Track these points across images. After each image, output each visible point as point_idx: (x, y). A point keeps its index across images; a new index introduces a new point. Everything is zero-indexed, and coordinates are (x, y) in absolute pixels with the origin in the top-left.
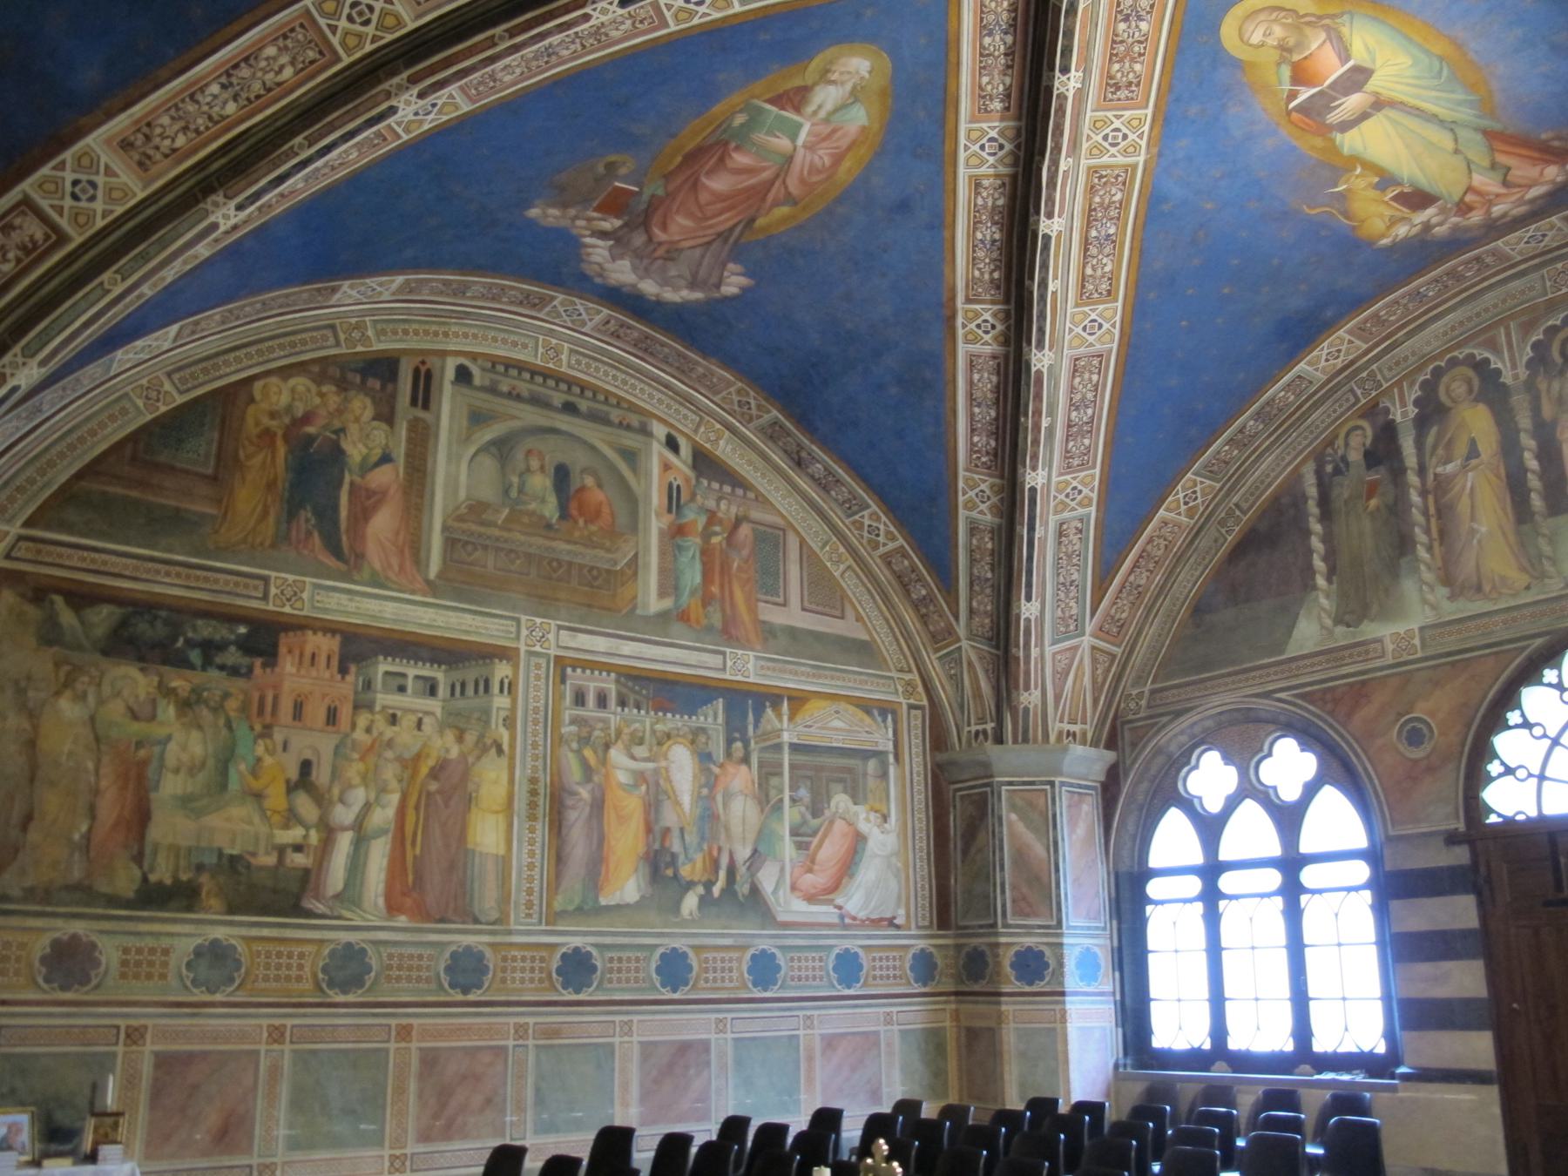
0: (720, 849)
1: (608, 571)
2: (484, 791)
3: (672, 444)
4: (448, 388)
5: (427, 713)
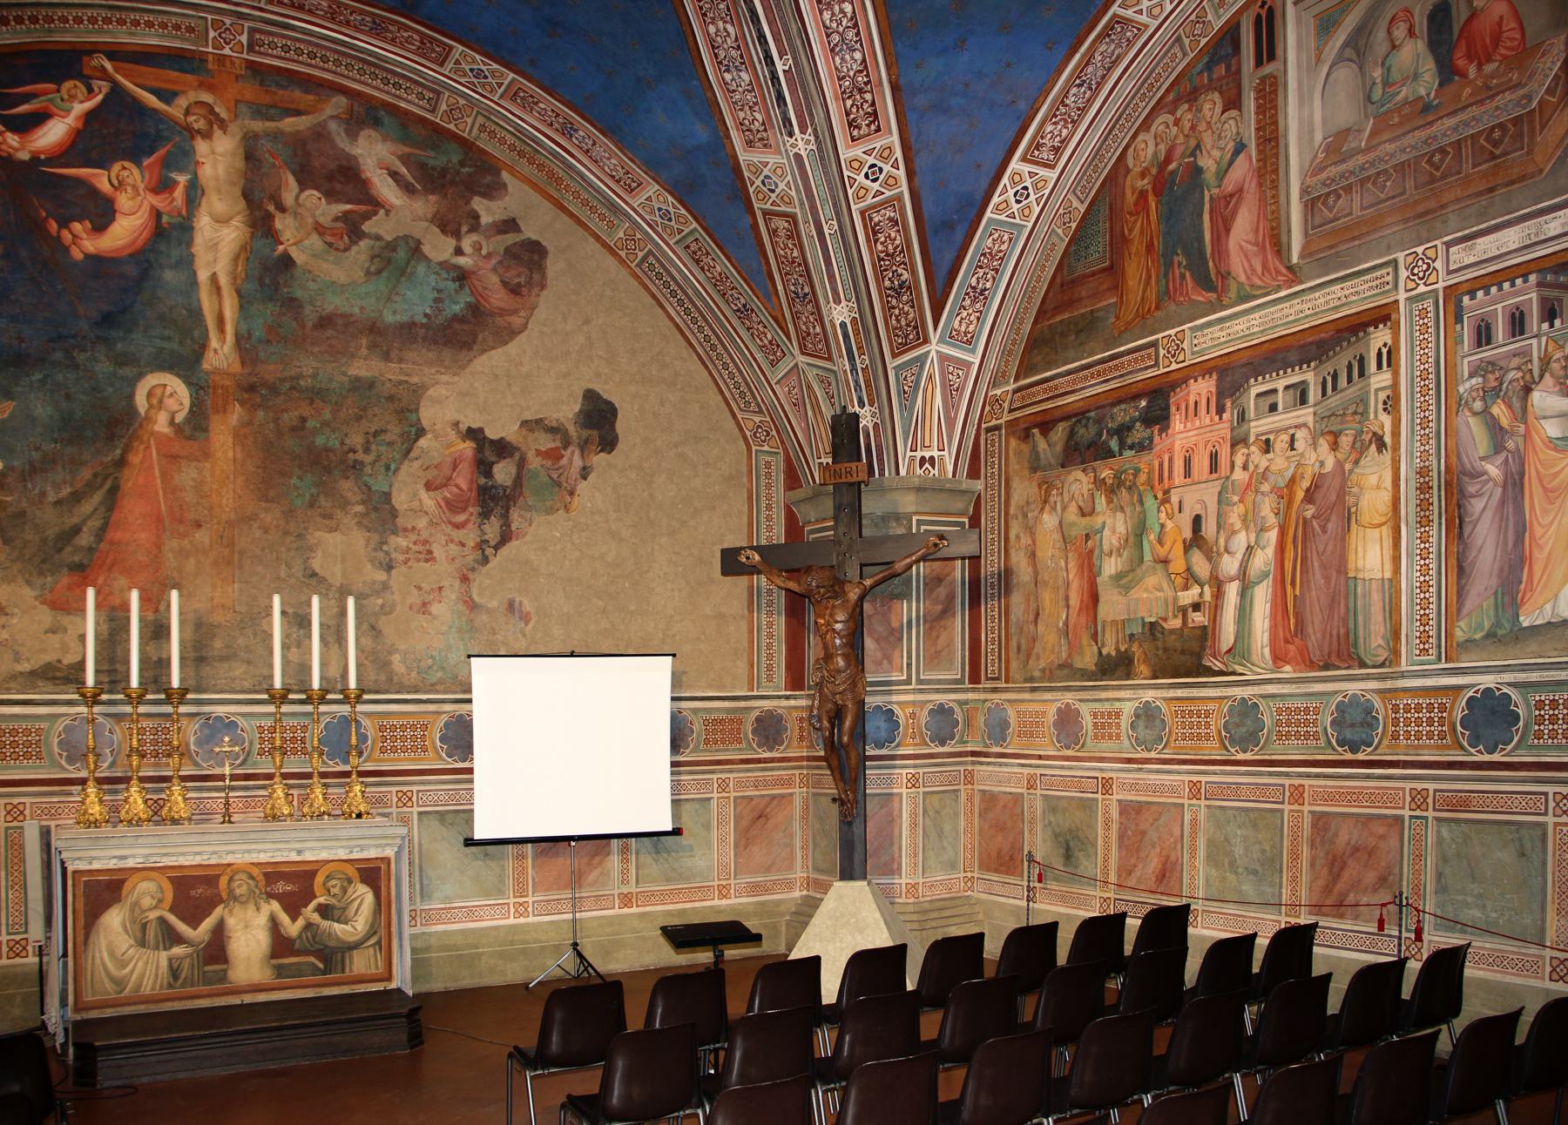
2: (1365, 502)
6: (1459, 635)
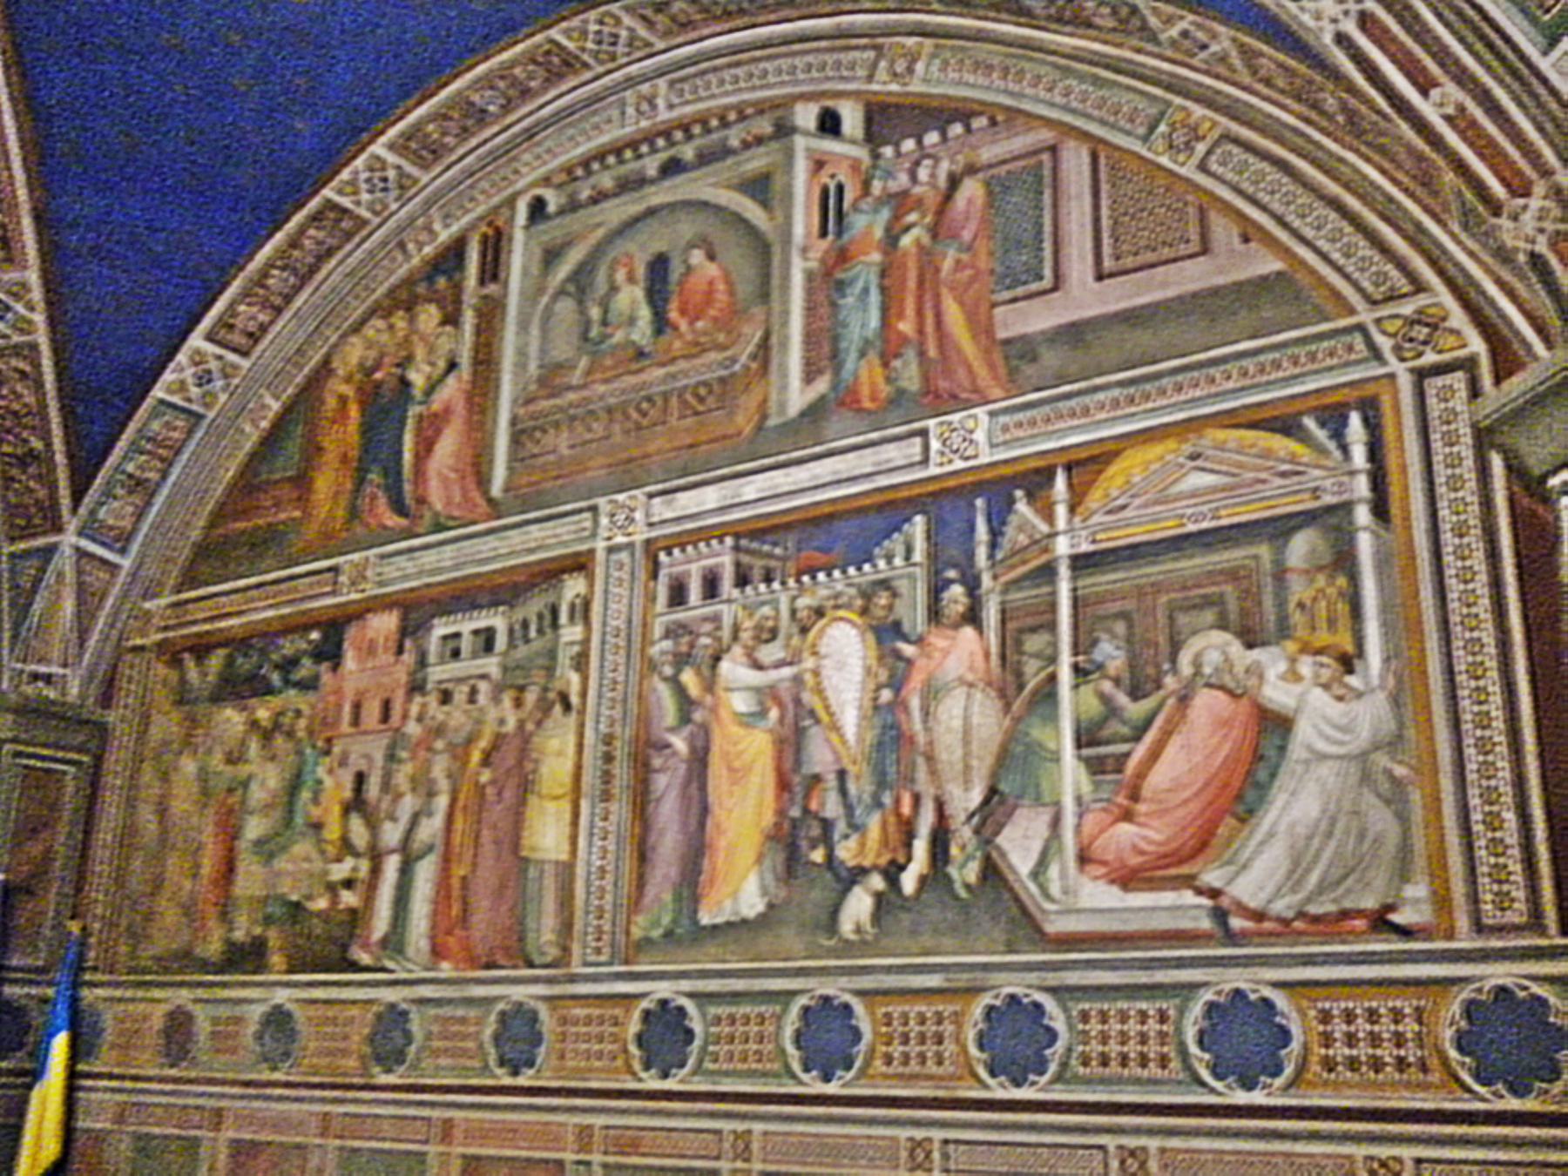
0: (917, 800)
1: (722, 380)
2: (544, 770)
3: (830, 124)
4: (519, 235)
5: (484, 677)
6: (637, 933)
